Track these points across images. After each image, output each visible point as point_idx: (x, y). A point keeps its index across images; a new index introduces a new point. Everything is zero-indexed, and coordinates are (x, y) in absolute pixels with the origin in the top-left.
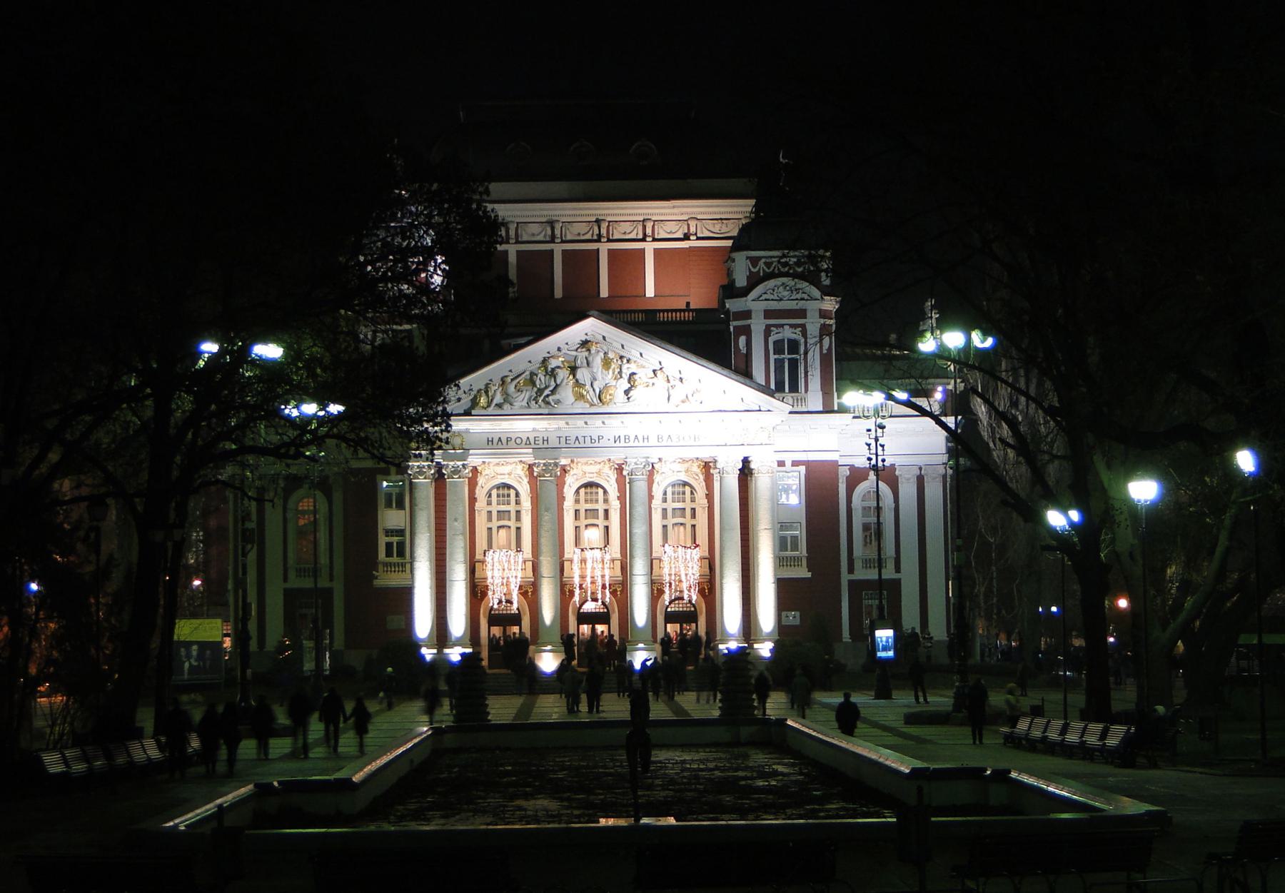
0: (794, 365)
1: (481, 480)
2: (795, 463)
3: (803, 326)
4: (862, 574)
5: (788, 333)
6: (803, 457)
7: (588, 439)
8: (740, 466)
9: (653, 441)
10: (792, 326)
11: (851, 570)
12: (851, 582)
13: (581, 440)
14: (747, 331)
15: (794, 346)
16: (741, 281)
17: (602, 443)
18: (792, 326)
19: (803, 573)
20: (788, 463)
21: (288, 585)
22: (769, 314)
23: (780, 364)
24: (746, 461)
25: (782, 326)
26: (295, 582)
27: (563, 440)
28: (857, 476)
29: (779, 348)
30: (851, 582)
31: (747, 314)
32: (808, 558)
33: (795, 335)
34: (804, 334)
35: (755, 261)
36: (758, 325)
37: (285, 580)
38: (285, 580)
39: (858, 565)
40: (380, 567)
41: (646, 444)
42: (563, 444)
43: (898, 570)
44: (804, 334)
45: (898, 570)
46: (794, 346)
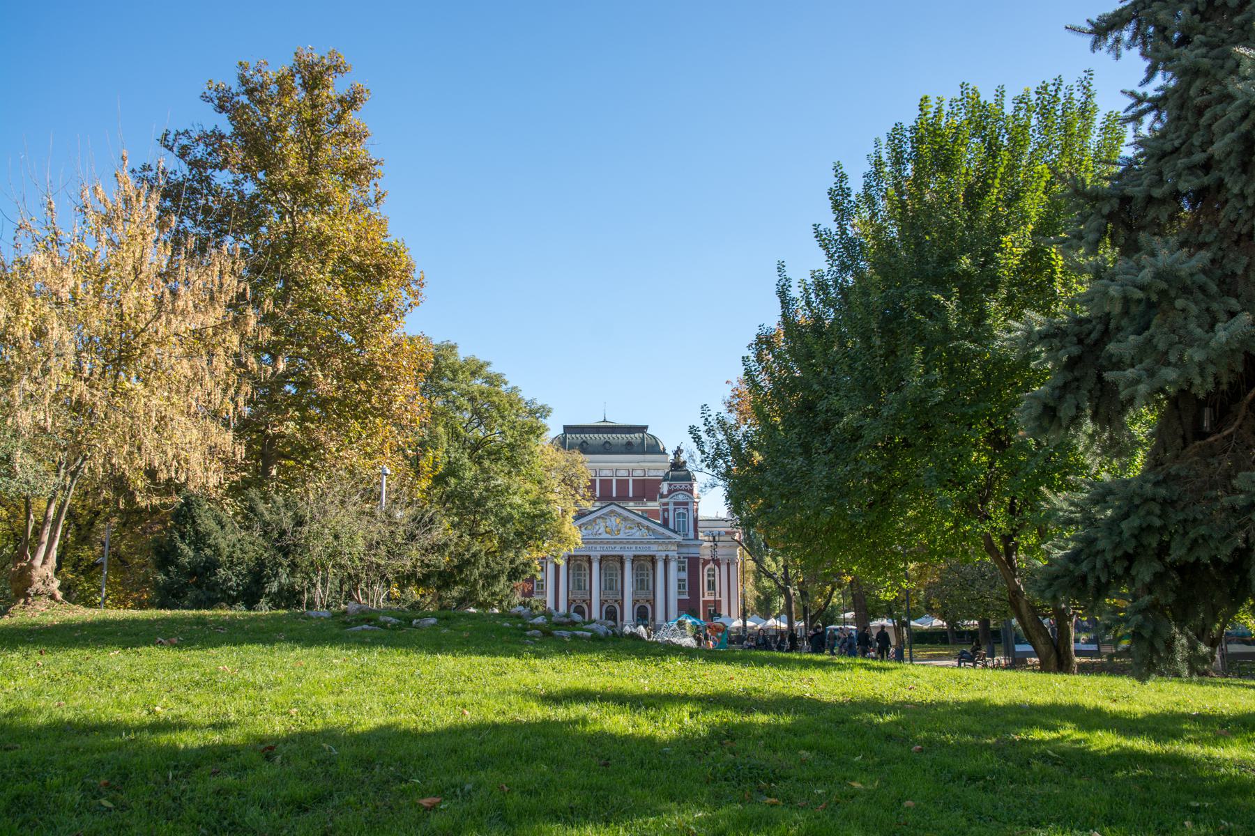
4: (707, 598)
14: (667, 510)
16: (665, 492)
19: (686, 597)
22: (675, 504)
28: (706, 562)
31: (667, 504)
36: (671, 507)
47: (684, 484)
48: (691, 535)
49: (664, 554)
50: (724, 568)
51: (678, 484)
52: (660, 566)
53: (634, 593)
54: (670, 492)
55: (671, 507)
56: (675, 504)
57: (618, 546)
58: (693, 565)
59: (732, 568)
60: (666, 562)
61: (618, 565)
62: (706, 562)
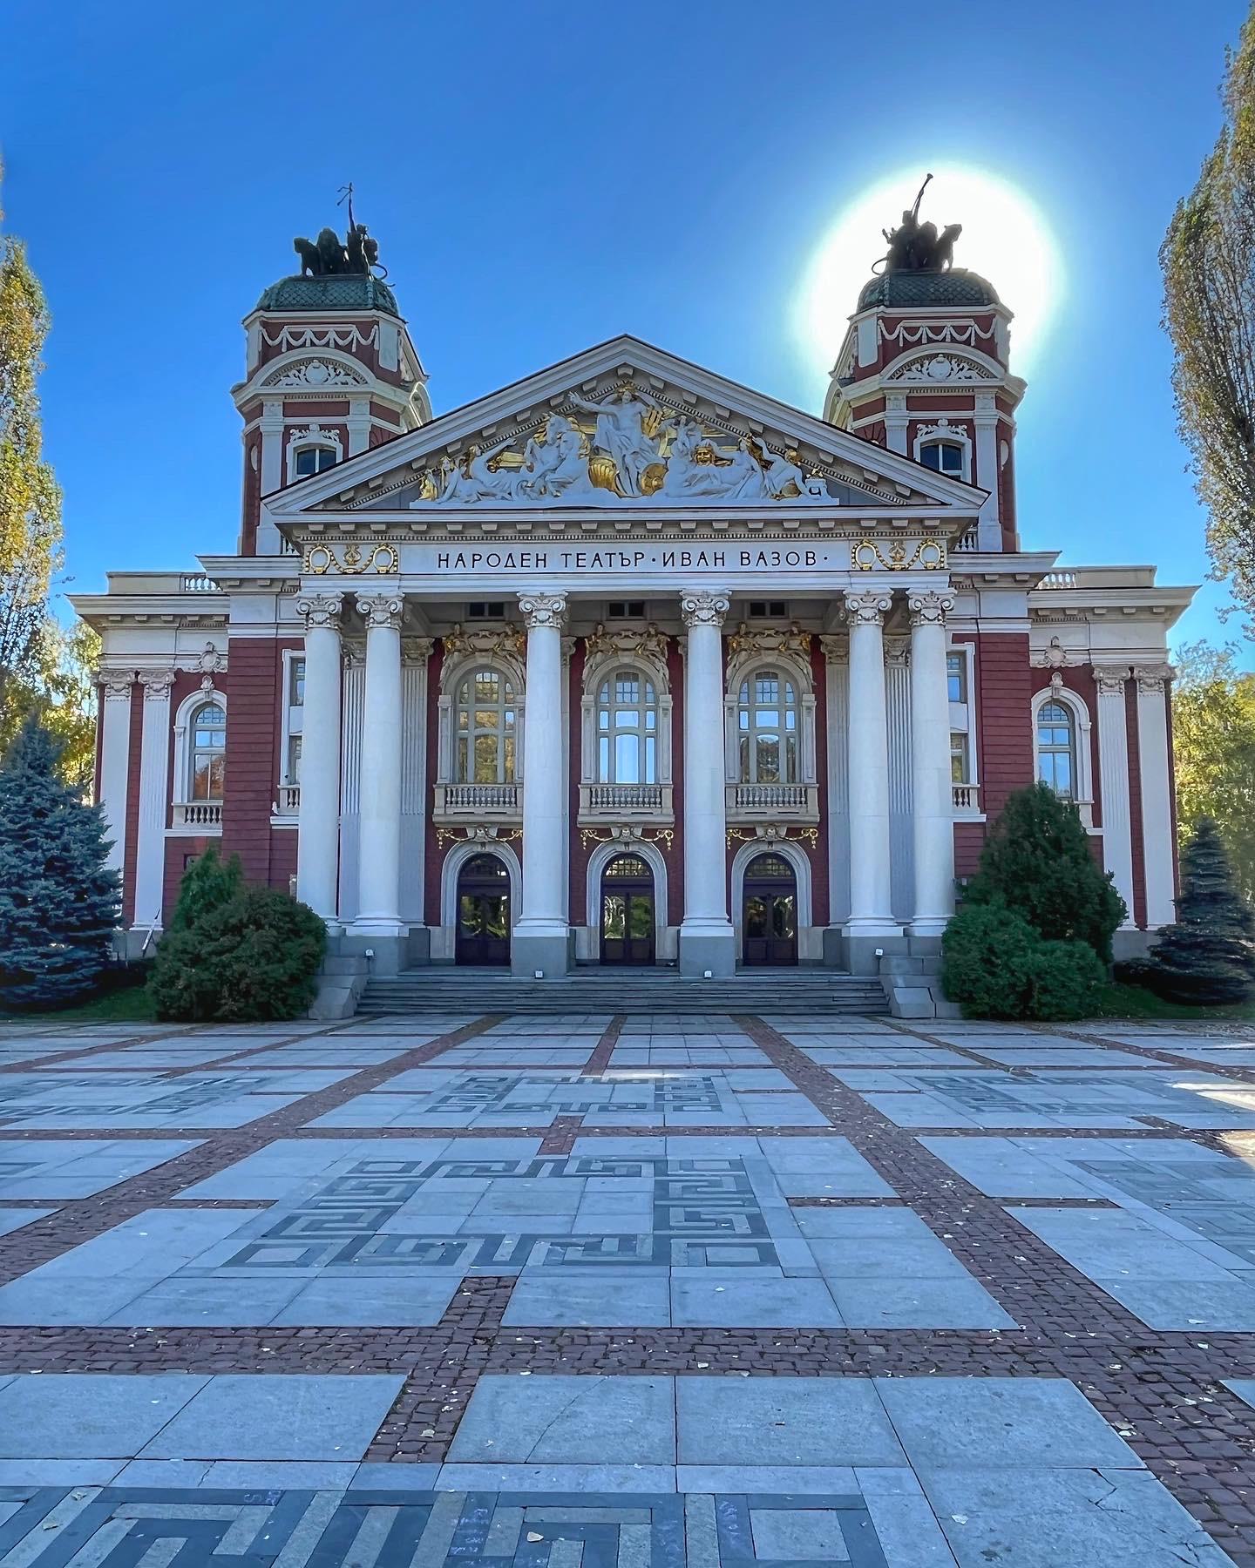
1: (449, 661)
2: (958, 638)
3: (970, 423)
5: (943, 432)
6: (970, 628)
7: (617, 559)
8: (887, 604)
9: (732, 563)
13: (605, 559)
15: (953, 455)
16: (868, 357)
17: (642, 566)
18: (952, 422)
21: (171, 833)
24: (900, 597)
25: (935, 422)
26: (182, 829)
27: (572, 560)
31: (880, 405)
34: (971, 433)
35: (891, 324)
36: (896, 417)
37: (169, 825)
38: (169, 825)
40: (283, 794)
41: (719, 567)
42: (572, 568)
43: (1097, 822)
44: (971, 433)
45: (1097, 822)
46: (953, 455)
47: (950, 316)
48: (989, 534)
50: (1111, 704)
51: (920, 317)
53: (736, 791)
54: (888, 352)
55: (896, 417)
56: (913, 403)
57: (653, 549)
58: (1003, 677)
59: (1150, 704)
60: (899, 617)
61: (660, 672)
62: (1042, 678)
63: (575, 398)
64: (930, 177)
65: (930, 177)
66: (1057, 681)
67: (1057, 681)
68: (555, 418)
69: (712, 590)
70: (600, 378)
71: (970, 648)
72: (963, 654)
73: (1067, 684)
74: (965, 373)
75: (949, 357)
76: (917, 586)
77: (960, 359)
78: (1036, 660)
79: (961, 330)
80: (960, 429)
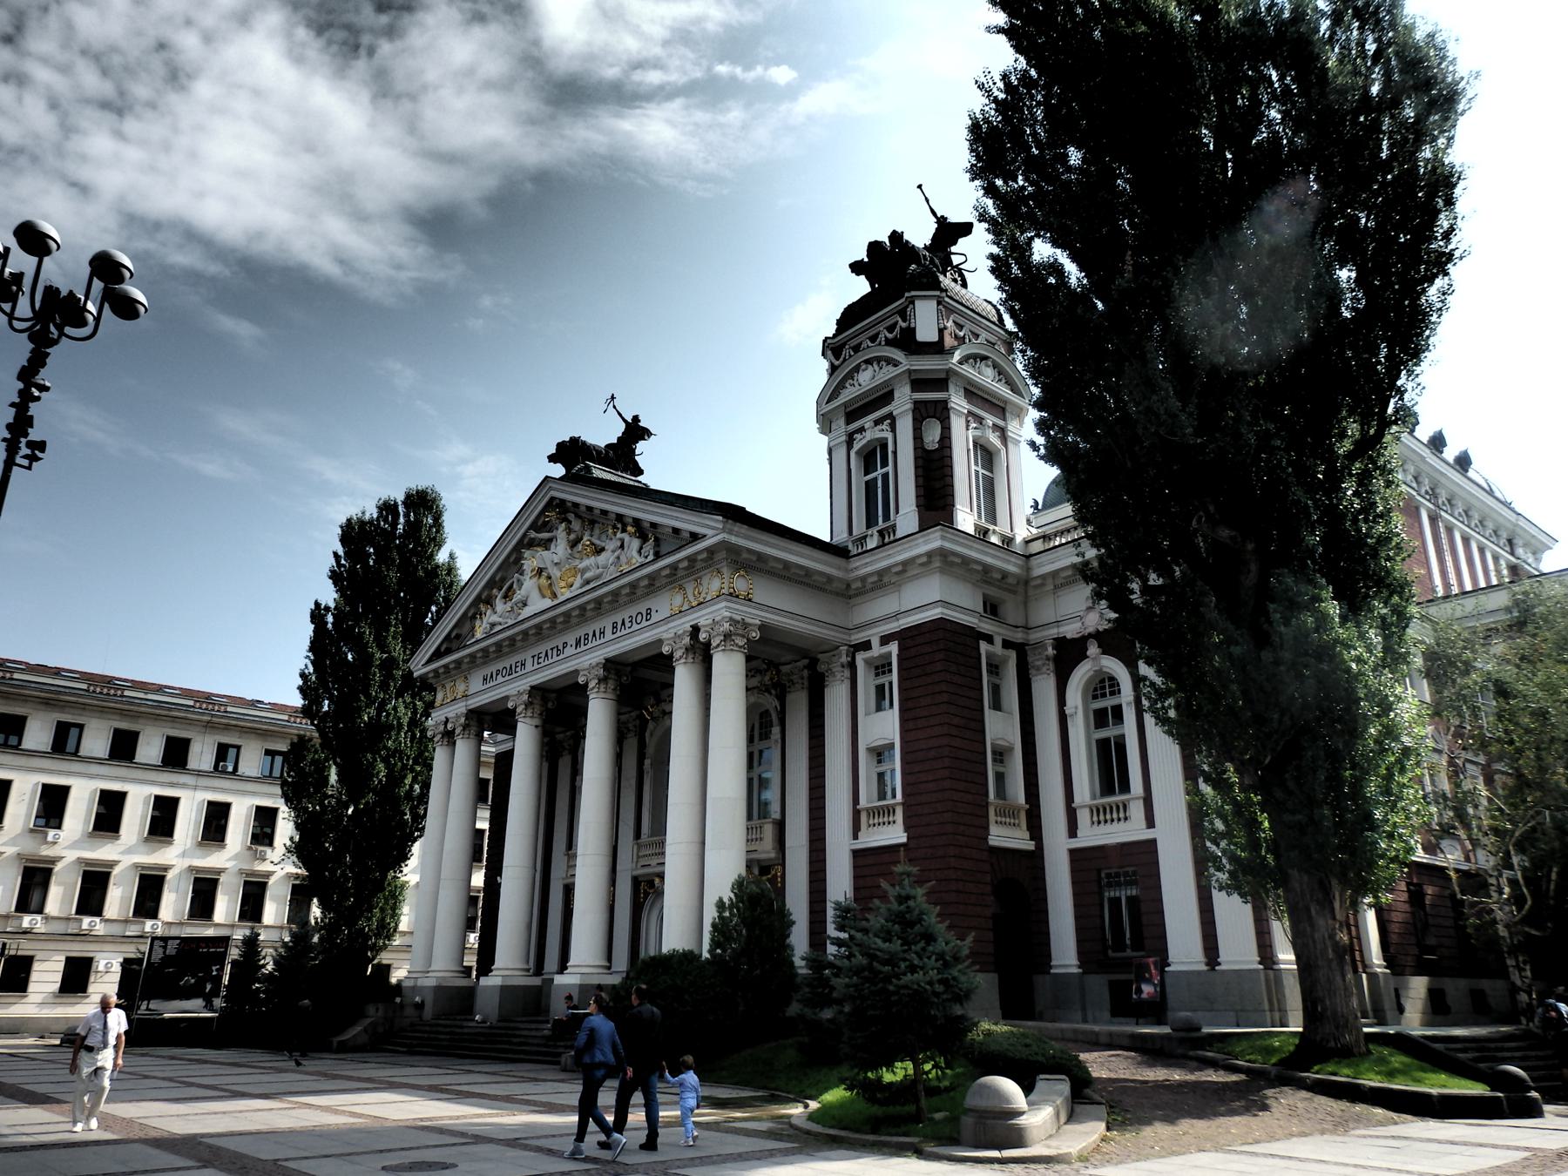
0: (885, 476)
3: (891, 417)
4: (1092, 835)
5: (873, 434)
8: (687, 640)
10: (877, 422)
11: (1073, 831)
12: (1078, 858)
19: (893, 834)
20: (875, 642)
23: (870, 487)
24: (696, 630)
29: (869, 466)
30: (1073, 853)
32: (906, 805)
33: (883, 432)
39: (1083, 817)
43: (1150, 823)
45: (1150, 823)
49: (684, 624)
52: (684, 680)
63: (533, 534)
64: (920, 187)
65: (920, 187)
66: (1093, 650)
67: (1093, 650)
68: (527, 554)
69: (594, 661)
70: (542, 512)
71: (894, 648)
72: (890, 654)
73: (1107, 650)
74: (885, 369)
75: (868, 362)
76: (703, 618)
77: (879, 359)
78: (1071, 631)
79: (891, 329)
80: (885, 425)
